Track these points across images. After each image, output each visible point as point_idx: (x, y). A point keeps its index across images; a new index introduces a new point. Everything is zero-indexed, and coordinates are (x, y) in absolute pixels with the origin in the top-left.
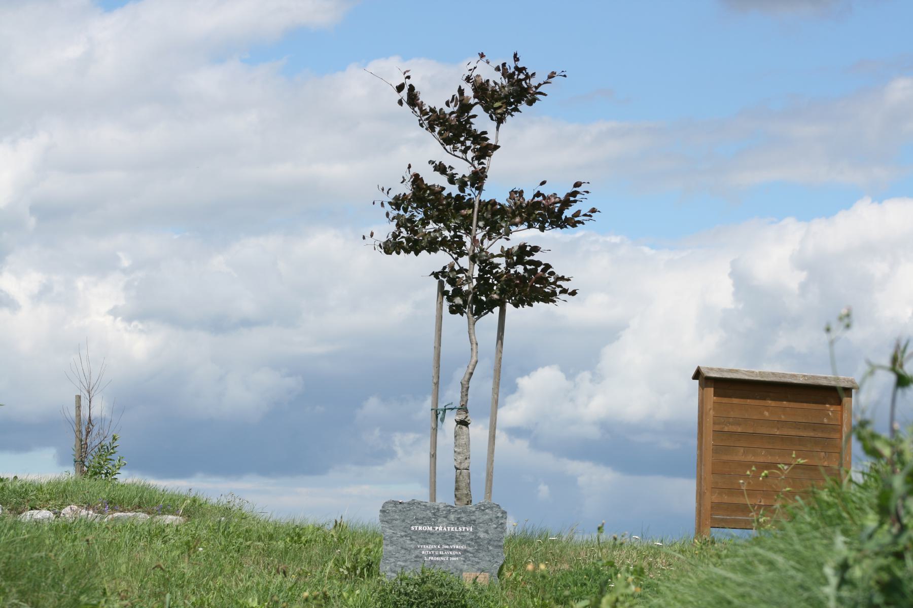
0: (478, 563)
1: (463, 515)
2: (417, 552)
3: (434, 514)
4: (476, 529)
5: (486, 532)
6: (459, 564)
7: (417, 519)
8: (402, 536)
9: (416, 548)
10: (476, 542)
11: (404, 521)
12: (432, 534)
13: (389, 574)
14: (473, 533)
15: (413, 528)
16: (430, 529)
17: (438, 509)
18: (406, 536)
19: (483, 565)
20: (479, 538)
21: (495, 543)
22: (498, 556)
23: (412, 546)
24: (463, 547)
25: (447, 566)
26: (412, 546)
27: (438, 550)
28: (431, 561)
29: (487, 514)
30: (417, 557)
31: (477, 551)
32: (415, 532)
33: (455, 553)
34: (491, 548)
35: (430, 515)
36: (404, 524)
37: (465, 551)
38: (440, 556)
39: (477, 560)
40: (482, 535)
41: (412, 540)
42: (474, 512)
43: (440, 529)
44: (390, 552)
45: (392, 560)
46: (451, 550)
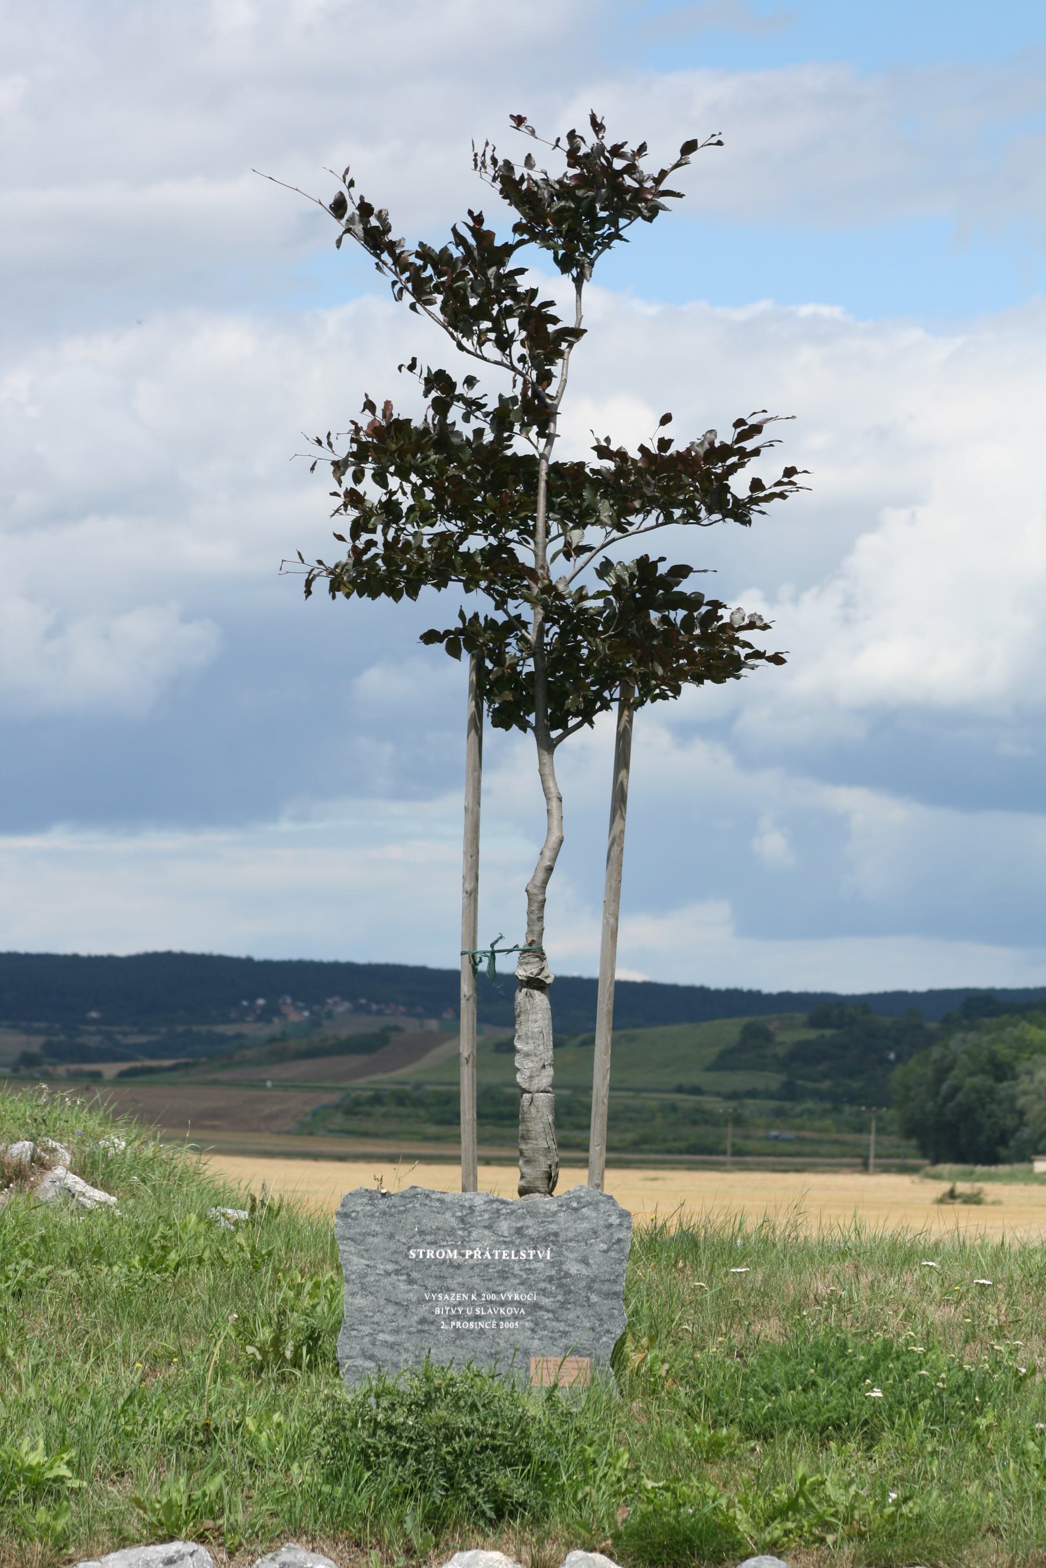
0: (565, 1334)
1: (529, 1221)
2: (423, 1309)
3: (462, 1220)
4: (560, 1253)
5: (584, 1261)
6: (523, 1339)
7: (421, 1233)
8: (388, 1274)
9: (421, 1301)
10: (560, 1286)
11: (391, 1236)
12: (459, 1267)
13: (359, 1362)
14: (553, 1264)
15: (412, 1254)
16: (453, 1255)
17: (471, 1208)
18: (397, 1272)
19: (580, 1337)
20: (567, 1275)
21: (606, 1287)
22: (611, 1316)
23: (413, 1297)
24: (530, 1297)
25: (494, 1342)
26: (413, 1297)
27: (472, 1304)
28: (456, 1330)
29: (584, 1218)
30: (423, 1321)
31: (563, 1305)
32: (417, 1262)
33: (511, 1311)
34: (594, 1298)
35: (453, 1222)
36: (392, 1245)
37: (536, 1306)
38: (477, 1318)
39: (561, 1326)
40: (573, 1268)
41: (411, 1281)
42: (554, 1214)
43: (477, 1254)
44: (360, 1310)
45: (366, 1329)
46: (502, 1304)
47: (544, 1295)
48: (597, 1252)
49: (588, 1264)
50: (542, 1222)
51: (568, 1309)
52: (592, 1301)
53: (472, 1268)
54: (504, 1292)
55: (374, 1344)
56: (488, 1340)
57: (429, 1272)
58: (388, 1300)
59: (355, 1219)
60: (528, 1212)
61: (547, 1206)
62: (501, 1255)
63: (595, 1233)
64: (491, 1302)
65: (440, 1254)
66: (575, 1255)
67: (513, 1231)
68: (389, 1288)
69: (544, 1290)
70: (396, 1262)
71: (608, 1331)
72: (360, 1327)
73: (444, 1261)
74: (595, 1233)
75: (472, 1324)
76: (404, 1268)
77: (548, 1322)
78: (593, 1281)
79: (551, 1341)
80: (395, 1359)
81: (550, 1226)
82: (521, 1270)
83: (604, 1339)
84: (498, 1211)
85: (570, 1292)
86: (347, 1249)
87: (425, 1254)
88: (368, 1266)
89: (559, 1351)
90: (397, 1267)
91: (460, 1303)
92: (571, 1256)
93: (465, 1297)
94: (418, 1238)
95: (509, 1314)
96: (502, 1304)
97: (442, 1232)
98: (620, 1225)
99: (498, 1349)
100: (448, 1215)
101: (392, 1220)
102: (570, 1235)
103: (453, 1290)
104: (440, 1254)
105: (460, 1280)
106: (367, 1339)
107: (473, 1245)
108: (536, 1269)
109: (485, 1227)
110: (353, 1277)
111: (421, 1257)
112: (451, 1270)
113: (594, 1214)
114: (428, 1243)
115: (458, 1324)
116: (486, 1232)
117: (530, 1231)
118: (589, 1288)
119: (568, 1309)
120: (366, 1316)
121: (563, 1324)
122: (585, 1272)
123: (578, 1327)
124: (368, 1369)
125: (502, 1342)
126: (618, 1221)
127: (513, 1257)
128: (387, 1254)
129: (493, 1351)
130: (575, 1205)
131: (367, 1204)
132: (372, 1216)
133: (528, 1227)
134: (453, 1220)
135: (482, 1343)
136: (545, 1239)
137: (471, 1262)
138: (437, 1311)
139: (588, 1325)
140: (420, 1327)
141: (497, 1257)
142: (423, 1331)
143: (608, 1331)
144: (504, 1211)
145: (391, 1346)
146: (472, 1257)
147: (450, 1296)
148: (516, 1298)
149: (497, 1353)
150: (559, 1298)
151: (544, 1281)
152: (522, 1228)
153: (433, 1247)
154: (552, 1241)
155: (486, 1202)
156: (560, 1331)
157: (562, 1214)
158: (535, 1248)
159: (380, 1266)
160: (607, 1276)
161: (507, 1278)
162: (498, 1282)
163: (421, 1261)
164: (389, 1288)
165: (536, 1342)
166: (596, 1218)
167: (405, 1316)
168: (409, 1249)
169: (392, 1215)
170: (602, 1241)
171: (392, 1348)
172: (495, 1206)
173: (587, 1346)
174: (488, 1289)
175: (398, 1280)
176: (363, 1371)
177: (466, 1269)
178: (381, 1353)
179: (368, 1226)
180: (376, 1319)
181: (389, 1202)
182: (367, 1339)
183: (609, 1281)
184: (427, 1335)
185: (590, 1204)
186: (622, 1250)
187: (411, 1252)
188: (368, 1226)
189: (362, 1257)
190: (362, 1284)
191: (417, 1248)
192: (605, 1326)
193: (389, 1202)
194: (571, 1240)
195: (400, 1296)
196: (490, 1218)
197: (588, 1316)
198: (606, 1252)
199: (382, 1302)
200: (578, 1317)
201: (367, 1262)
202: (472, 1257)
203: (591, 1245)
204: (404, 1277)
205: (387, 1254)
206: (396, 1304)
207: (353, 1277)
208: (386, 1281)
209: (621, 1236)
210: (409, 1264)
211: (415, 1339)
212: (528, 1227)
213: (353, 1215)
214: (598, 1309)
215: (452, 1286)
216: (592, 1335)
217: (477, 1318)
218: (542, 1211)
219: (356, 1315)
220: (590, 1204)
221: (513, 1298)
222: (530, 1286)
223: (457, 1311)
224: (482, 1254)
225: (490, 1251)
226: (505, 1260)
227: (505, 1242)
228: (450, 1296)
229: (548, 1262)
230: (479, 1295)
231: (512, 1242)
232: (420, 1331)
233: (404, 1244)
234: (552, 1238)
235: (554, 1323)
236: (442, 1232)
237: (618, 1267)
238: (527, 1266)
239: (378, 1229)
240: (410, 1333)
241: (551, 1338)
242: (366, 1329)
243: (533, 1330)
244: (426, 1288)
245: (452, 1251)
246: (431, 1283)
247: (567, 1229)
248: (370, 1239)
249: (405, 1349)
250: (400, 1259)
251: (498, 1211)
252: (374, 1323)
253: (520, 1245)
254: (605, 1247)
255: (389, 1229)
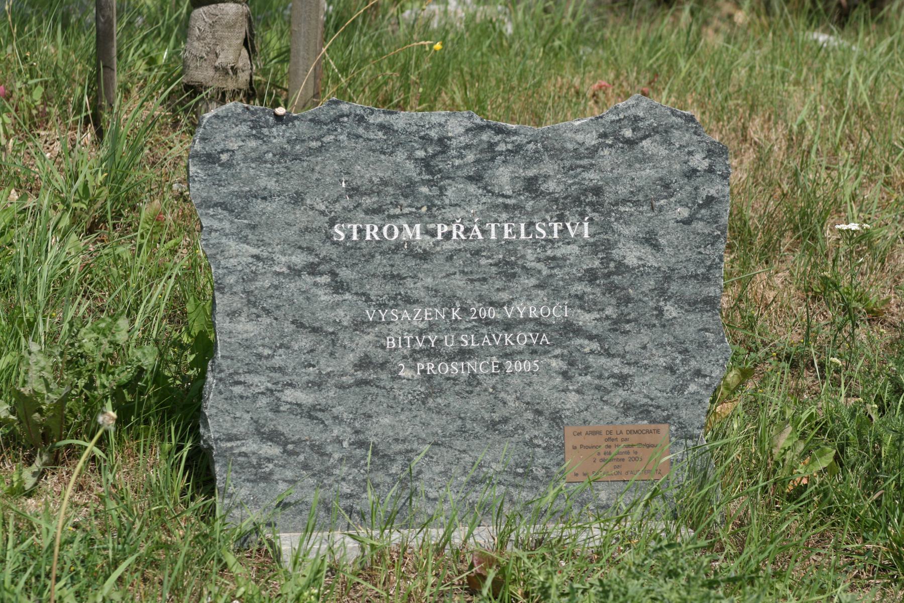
0: (622, 380)
1: (549, 167)
2: (364, 343)
3: (426, 164)
4: (606, 227)
5: (650, 240)
6: (547, 390)
7: (354, 191)
8: (295, 272)
9: (359, 325)
10: (611, 289)
11: (297, 199)
12: (425, 256)
13: (251, 446)
14: (594, 247)
15: (339, 232)
16: (414, 233)
17: (442, 142)
18: (312, 269)
19: (648, 386)
20: (621, 268)
21: (690, 289)
22: (703, 344)
23: (344, 316)
24: (558, 313)
25: (498, 401)
26: (344, 316)
27: (454, 327)
28: (428, 378)
29: (645, 159)
30: (364, 363)
31: (617, 325)
32: (349, 248)
33: (524, 338)
34: (671, 310)
35: (412, 170)
36: (301, 217)
37: (569, 329)
38: (463, 354)
39: (615, 366)
40: (632, 255)
41: (339, 287)
42: (593, 151)
43: (457, 232)
44: (247, 345)
45: (260, 382)
46: (508, 326)
47: (581, 307)
48: (672, 224)
49: (656, 247)
50: (571, 168)
51: (626, 333)
52: (667, 316)
53: (450, 258)
54: (509, 303)
55: (276, 411)
56: (485, 397)
57: (370, 267)
58: (299, 324)
59: (228, 165)
60: (546, 148)
61: (580, 137)
62: (500, 231)
63: (667, 186)
64: (488, 322)
65: (391, 234)
66: (634, 228)
67: (519, 185)
68: (299, 299)
69: (580, 298)
70: (310, 250)
71: (698, 373)
72: (249, 378)
73: (398, 246)
74: (667, 186)
75: (454, 366)
76: (326, 260)
77: (591, 359)
78: (668, 278)
79: (598, 395)
80: (317, 438)
81: (586, 175)
82: (539, 260)
83: (692, 388)
84: (491, 146)
85: (628, 300)
86: (216, 224)
87: (361, 231)
88: (257, 257)
89: (614, 412)
90: (311, 259)
91: (431, 327)
92: (626, 231)
93: (440, 313)
94: (347, 202)
95: (522, 345)
96: (508, 326)
97: (391, 190)
98: (710, 170)
99: (505, 412)
100: (401, 156)
101: (297, 166)
102: (623, 191)
103: (416, 302)
104: (391, 233)
105: (429, 281)
106: (263, 401)
107: (449, 213)
108: (564, 258)
109: (470, 178)
110: (231, 279)
111: (355, 237)
112: (412, 263)
113: (663, 152)
114: (367, 212)
115: (430, 367)
116: (472, 188)
117: (551, 186)
118: (661, 292)
119: (626, 333)
120: (260, 356)
121: (617, 360)
122: (652, 262)
123: (646, 367)
124: (269, 460)
125: (510, 399)
126: (706, 164)
127: (523, 236)
128: (291, 234)
129: (496, 417)
130: (628, 133)
131: (249, 136)
132: (260, 160)
133: (547, 177)
134: (410, 165)
135: (474, 402)
136: (577, 201)
137: (447, 246)
138: (390, 343)
139: (662, 362)
140: (359, 374)
141: (493, 236)
142: (366, 382)
143: (698, 373)
144: (502, 147)
145: (311, 413)
146: (448, 236)
147: (412, 313)
148: (533, 314)
149: (505, 420)
150: (609, 311)
151: (580, 279)
152: (535, 178)
153: (376, 218)
154: (591, 204)
155: (468, 130)
156: (613, 376)
157: (606, 152)
158: (561, 218)
159: (278, 257)
160: (692, 268)
161: (514, 275)
162: (499, 284)
163: (356, 246)
164: (299, 299)
165: (573, 397)
166: (668, 157)
167: (332, 354)
168: (332, 223)
169: (296, 158)
170: (679, 202)
171: (311, 417)
172: (485, 137)
173: (662, 402)
174: (480, 298)
175: (316, 284)
176: (259, 466)
177: (439, 260)
178: (294, 427)
179: (253, 179)
180: (277, 361)
181: (291, 133)
182: (263, 401)
183: (696, 276)
184: (374, 390)
185: (655, 131)
186: (715, 219)
187: (336, 229)
188: (253, 179)
189: (245, 240)
190: (249, 293)
191: (346, 220)
192: (693, 363)
193: (291, 133)
194: (624, 202)
195: (320, 315)
196: (478, 161)
197: (662, 345)
198: (687, 222)
199: (289, 328)
200: (644, 347)
201: (255, 251)
202: (448, 236)
203: (661, 209)
204: (325, 279)
205: (291, 234)
206: (315, 330)
207: (231, 279)
208: (292, 286)
209: (713, 192)
210: (334, 252)
211: (352, 398)
212: (547, 177)
213: (224, 157)
214: (678, 331)
215: (416, 294)
216: (670, 380)
217: (463, 354)
218: (570, 146)
219: (241, 353)
220: (655, 131)
221: (526, 313)
222: (557, 290)
223: (427, 341)
224: (467, 231)
225: (482, 224)
226: (508, 242)
227: (506, 207)
228: (412, 313)
229: (587, 243)
230: (464, 310)
231: (518, 207)
232: (360, 383)
233: (322, 213)
234: (591, 198)
235: (603, 360)
236: (391, 190)
237: (709, 250)
238: (549, 253)
239: (272, 184)
240: (342, 387)
241: (598, 388)
242: (260, 382)
243: (565, 375)
244: (368, 299)
245: (411, 226)
246: (376, 289)
247: (616, 180)
248: (259, 205)
249: (335, 418)
250: (317, 243)
251: (491, 146)
252: (273, 369)
253: (534, 212)
254: (685, 213)
255: (293, 185)
